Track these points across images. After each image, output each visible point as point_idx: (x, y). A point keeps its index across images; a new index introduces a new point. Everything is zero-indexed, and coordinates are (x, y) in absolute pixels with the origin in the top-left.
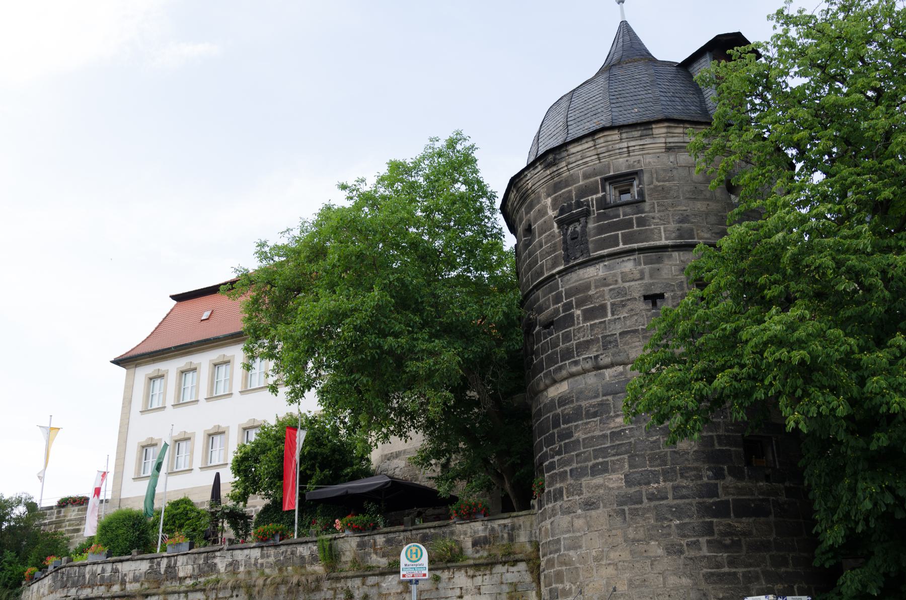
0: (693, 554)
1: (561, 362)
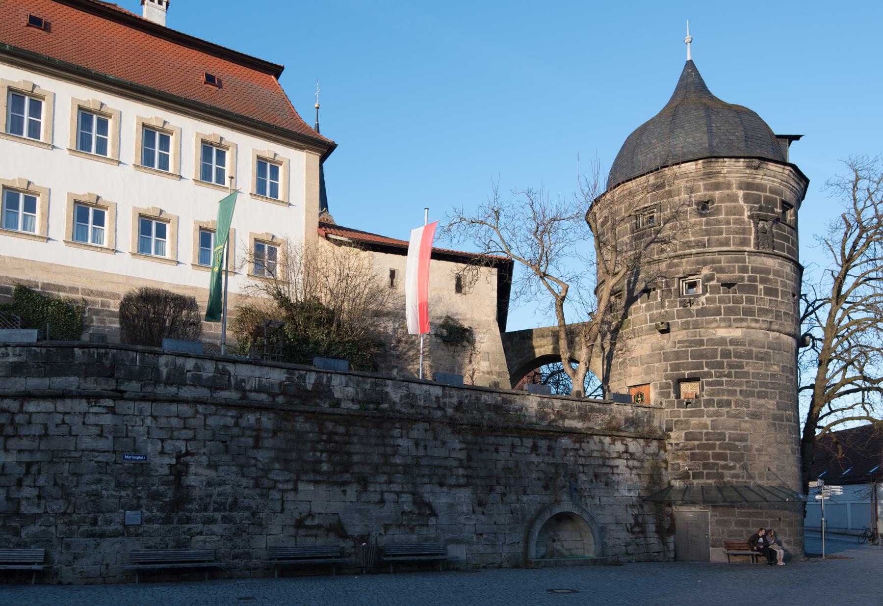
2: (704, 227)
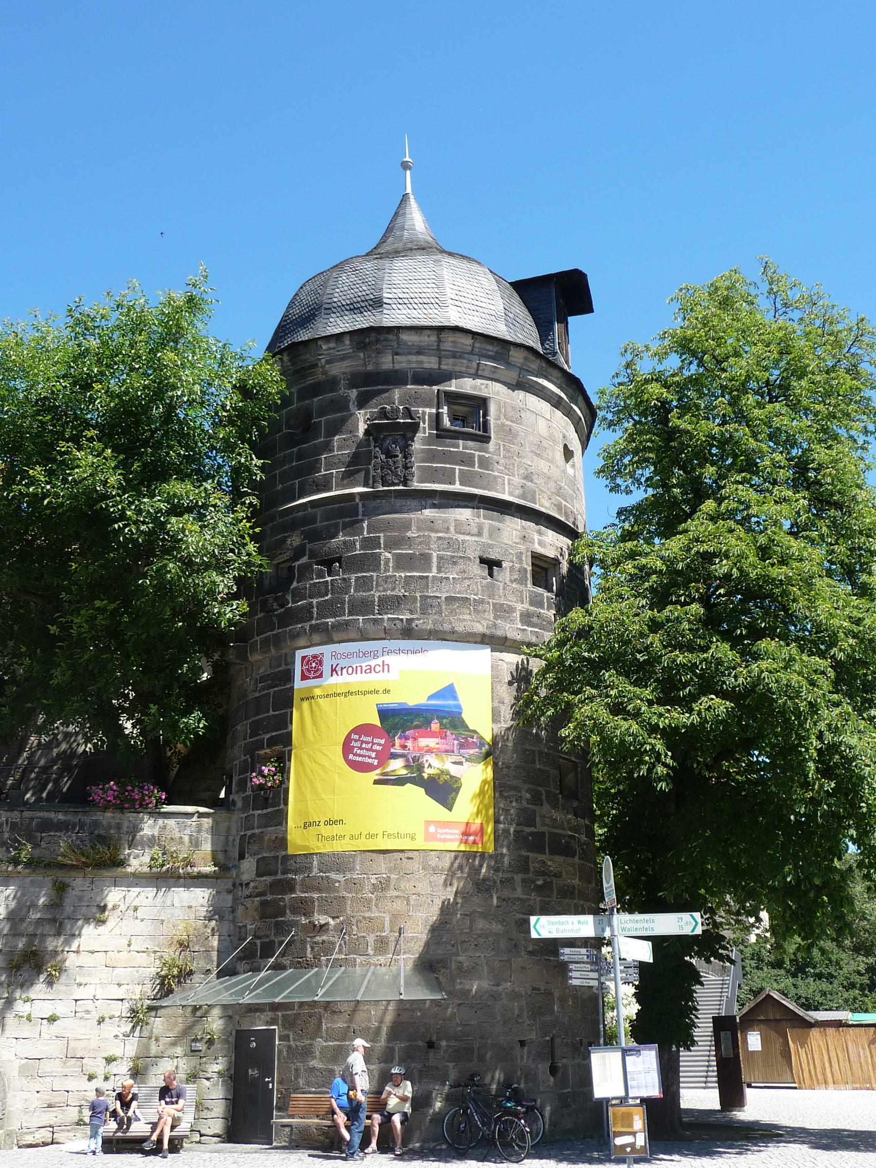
0: (506, 894)
1: (350, 614)
2: (294, 464)
